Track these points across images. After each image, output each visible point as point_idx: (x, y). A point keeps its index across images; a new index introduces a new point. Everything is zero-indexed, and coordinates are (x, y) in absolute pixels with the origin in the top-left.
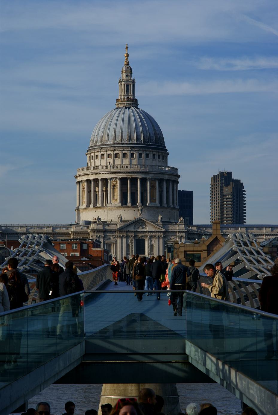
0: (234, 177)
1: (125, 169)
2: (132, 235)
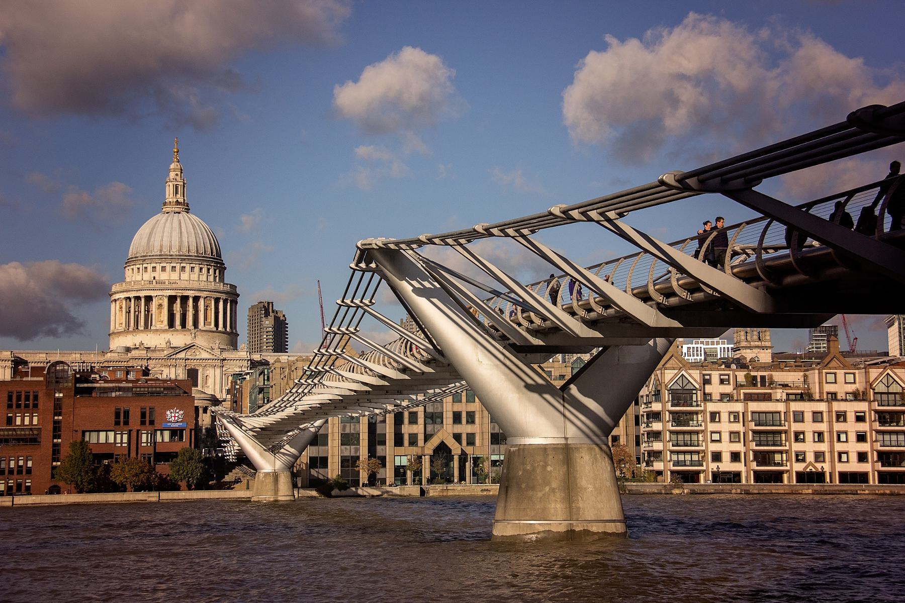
1: (174, 286)
2: (183, 363)
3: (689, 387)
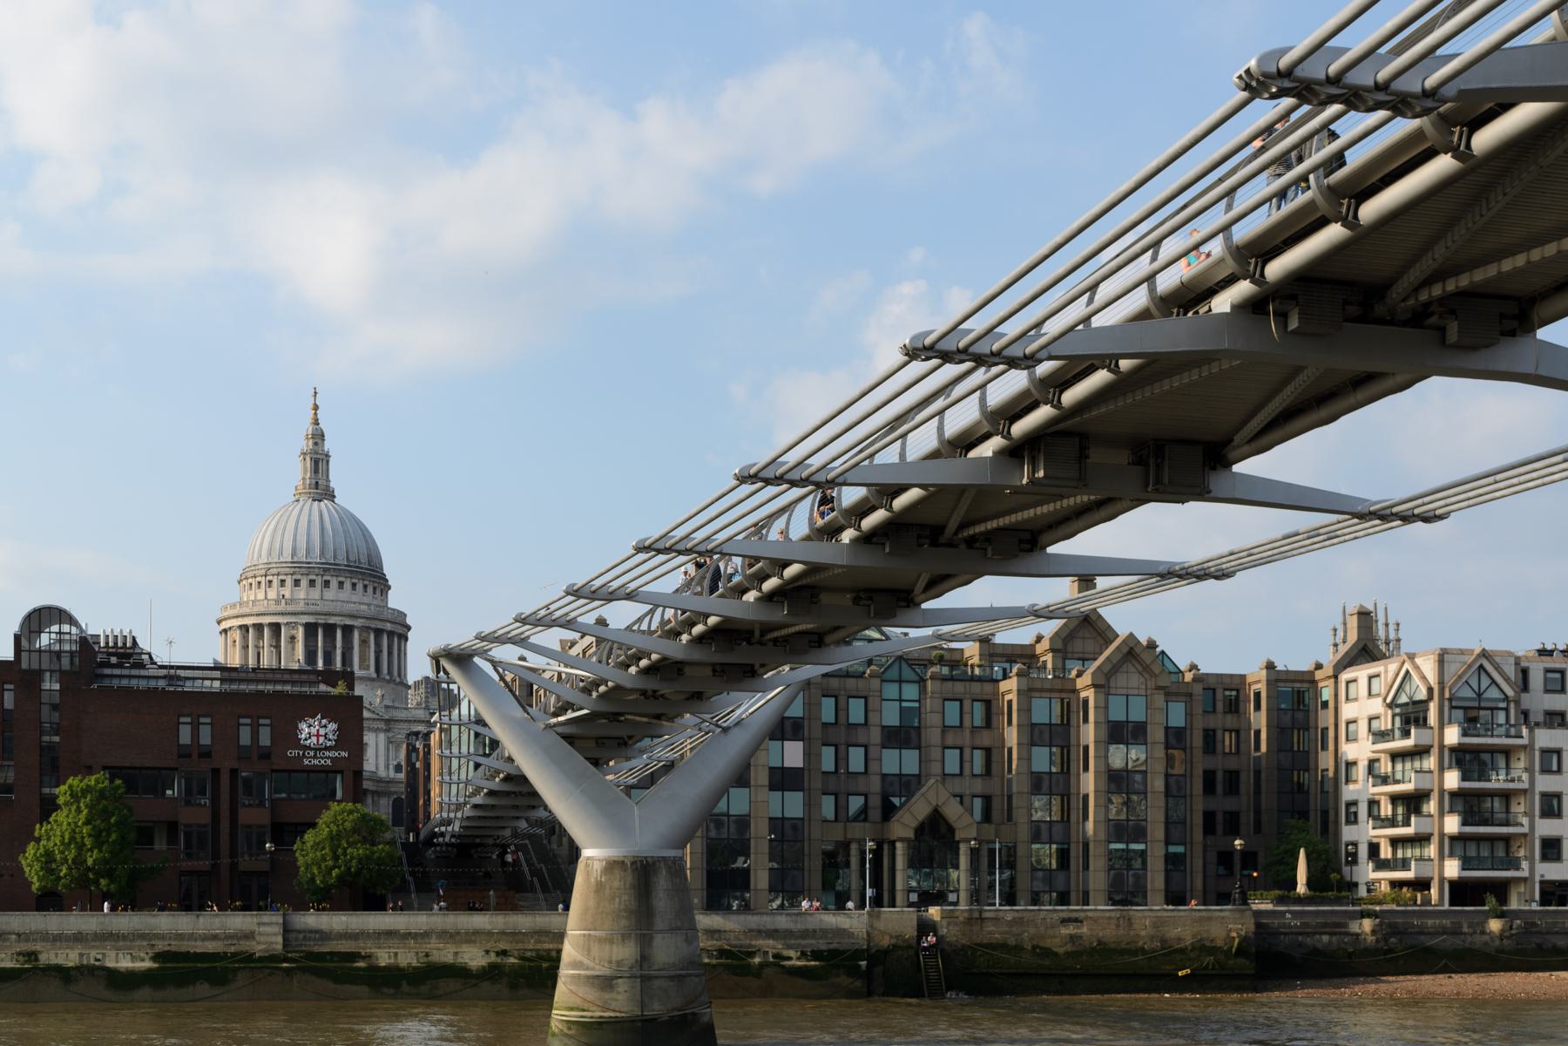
1: (312, 608)
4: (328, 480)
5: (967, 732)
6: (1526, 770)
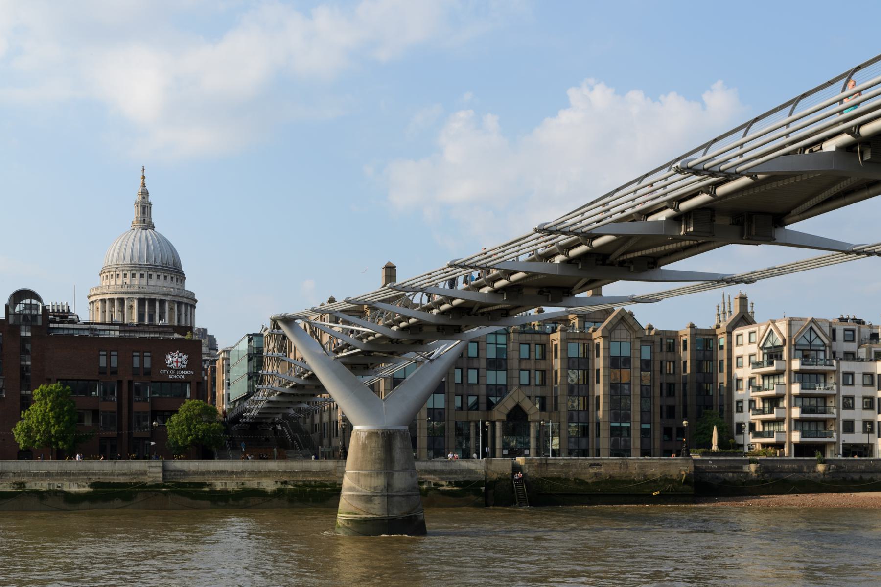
0: (209, 333)
1: (142, 290)
3: (818, 342)
4: (151, 218)
5: (533, 362)
6: (835, 383)
